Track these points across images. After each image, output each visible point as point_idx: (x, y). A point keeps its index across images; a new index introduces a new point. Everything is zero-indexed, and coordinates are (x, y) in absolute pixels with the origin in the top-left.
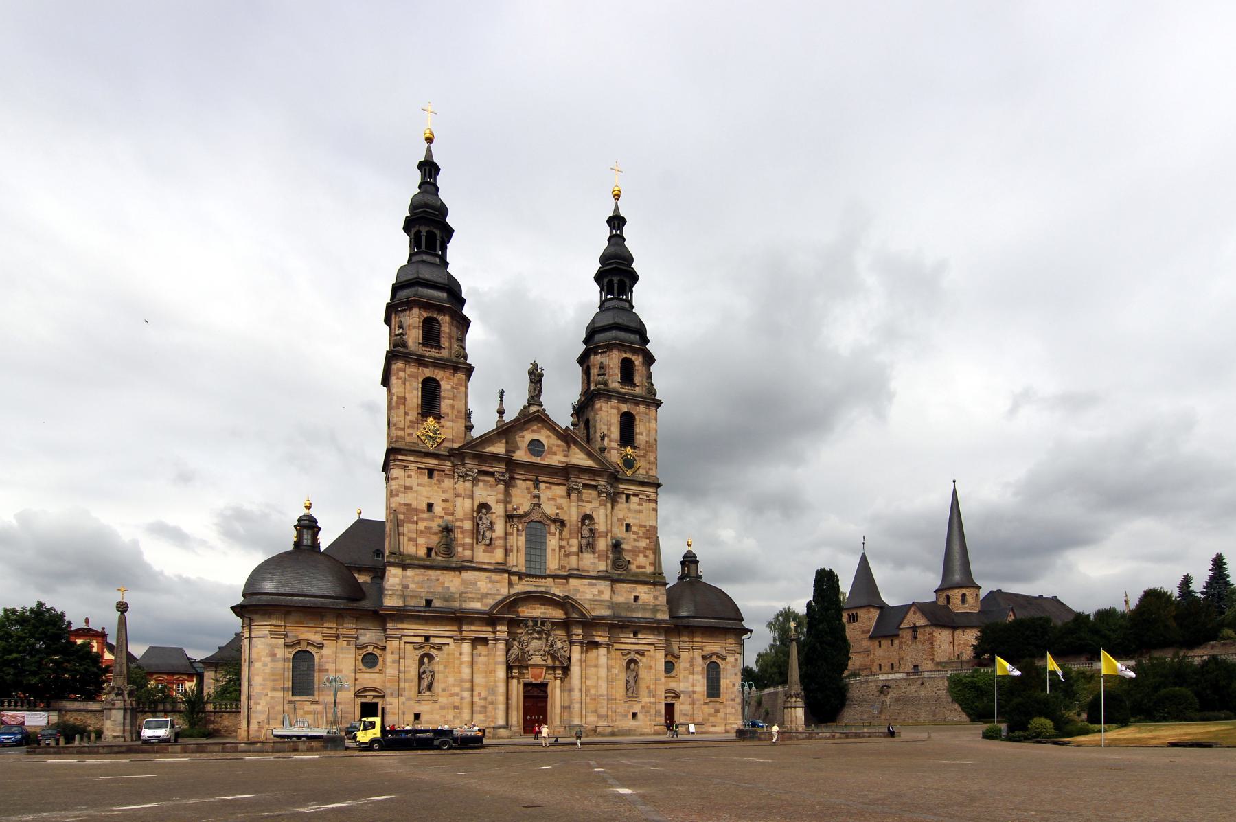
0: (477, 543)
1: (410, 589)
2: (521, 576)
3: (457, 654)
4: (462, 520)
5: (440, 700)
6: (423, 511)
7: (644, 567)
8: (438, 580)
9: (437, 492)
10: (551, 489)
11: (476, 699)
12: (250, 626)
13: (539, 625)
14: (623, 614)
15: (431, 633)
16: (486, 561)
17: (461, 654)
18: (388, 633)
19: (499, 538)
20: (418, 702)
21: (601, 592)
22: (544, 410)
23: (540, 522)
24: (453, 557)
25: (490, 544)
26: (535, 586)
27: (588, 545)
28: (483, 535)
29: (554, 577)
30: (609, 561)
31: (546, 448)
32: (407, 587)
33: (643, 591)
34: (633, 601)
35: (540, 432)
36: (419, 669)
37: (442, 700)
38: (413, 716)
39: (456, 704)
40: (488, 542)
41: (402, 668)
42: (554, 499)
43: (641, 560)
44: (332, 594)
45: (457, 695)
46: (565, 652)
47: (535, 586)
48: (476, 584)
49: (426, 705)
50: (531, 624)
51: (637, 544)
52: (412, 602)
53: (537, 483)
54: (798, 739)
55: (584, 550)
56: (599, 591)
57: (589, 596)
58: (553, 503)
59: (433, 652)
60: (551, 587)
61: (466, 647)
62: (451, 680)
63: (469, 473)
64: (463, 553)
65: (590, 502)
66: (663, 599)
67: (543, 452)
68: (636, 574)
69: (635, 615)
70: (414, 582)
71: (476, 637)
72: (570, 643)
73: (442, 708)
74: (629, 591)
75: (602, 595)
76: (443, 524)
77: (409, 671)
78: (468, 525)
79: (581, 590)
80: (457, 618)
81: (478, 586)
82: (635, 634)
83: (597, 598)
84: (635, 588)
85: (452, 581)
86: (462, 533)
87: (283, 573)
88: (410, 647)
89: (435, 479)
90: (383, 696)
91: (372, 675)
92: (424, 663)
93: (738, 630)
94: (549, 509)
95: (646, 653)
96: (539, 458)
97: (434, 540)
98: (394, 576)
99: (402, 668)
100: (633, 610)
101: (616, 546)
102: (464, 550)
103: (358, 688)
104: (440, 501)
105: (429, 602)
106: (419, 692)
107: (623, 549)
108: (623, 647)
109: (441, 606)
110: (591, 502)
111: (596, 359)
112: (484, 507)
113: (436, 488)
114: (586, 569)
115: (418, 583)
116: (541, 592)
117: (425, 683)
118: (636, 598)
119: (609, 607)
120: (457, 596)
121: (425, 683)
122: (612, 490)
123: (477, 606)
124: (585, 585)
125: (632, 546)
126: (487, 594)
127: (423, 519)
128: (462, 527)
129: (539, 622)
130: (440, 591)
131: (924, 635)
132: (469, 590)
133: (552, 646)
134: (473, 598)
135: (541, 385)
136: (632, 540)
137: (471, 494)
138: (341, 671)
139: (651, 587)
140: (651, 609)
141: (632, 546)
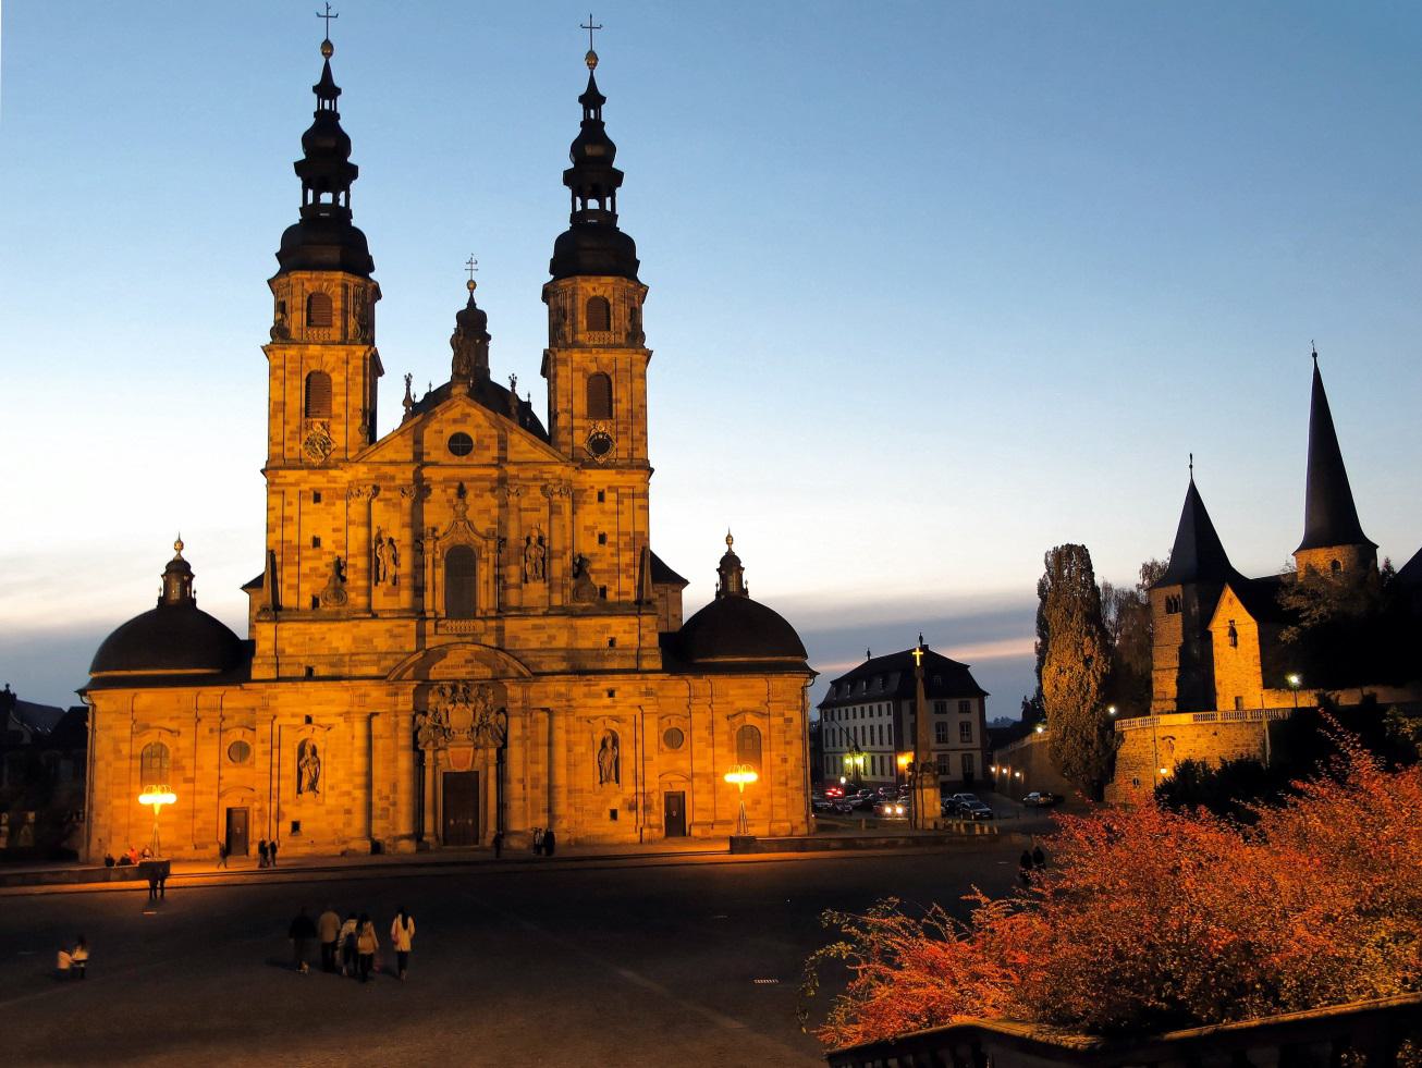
0: (376, 584)
3: (349, 738)
4: (354, 556)
6: (307, 548)
7: (628, 593)
8: (323, 639)
10: (482, 496)
11: (375, 798)
14: (590, 665)
17: (353, 737)
19: (405, 575)
20: (299, 805)
21: (552, 638)
24: (343, 605)
25: (394, 584)
26: (459, 635)
30: (568, 592)
31: (475, 442)
32: (283, 651)
33: (621, 629)
34: (606, 644)
35: (465, 422)
36: (299, 760)
37: (331, 801)
39: (346, 807)
40: (390, 583)
41: (275, 760)
47: (459, 635)
48: (372, 642)
50: (448, 691)
51: (615, 560)
52: (286, 672)
53: (461, 492)
56: (549, 637)
57: (534, 645)
58: (487, 516)
65: (538, 510)
70: (291, 645)
77: (286, 765)
78: (361, 563)
79: (522, 637)
82: (611, 694)
83: (548, 646)
85: (343, 639)
86: (355, 573)
89: (323, 503)
96: (465, 457)
97: (324, 582)
98: (265, 639)
99: (275, 760)
101: (580, 567)
102: (357, 595)
103: (222, 788)
105: (310, 670)
106: (300, 792)
107: (593, 571)
108: (593, 713)
109: (326, 674)
115: (296, 645)
116: (468, 643)
117: (306, 782)
118: (612, 642)
119: (564, 659)
120: (347, 659)
121: (306, 782)
123: (373, 671)
124: (527, 630)
126: (387, 653)
130: (327, 653)
132: (361, 650)
136: (608, 555)
137: (363, 519)
138: (201, 768)
139: (636, 620)
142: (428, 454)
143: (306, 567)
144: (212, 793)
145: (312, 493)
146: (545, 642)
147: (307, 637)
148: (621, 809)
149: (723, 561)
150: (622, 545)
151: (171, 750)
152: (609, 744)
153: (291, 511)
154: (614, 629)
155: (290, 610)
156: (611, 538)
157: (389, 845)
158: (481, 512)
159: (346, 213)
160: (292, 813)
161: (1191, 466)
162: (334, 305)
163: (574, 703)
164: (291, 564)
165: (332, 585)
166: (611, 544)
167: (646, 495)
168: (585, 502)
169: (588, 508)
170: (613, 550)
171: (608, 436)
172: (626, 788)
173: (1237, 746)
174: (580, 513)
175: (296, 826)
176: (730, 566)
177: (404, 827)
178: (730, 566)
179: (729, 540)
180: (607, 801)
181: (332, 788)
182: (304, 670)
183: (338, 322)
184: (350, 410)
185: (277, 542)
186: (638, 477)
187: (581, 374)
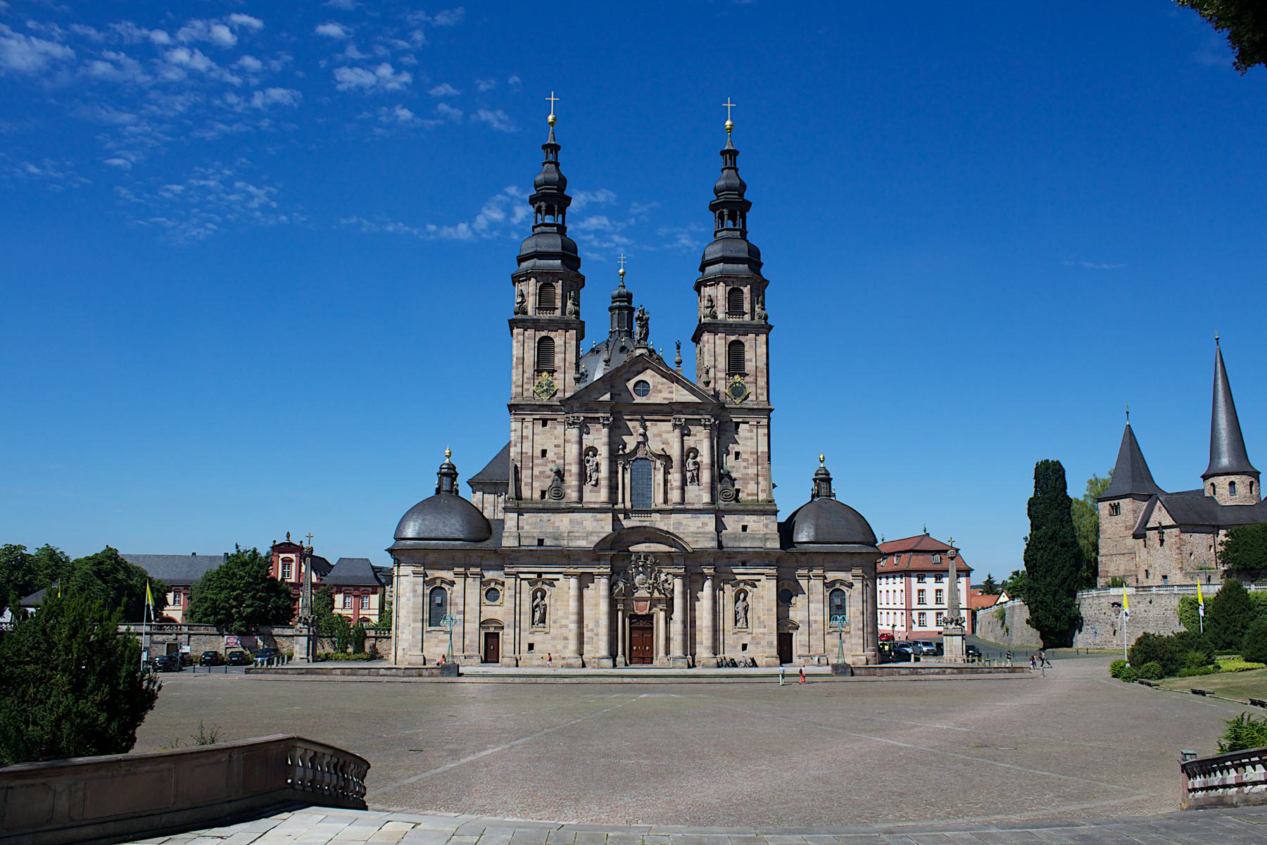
1: (525, 530)
2: (627, 513)
4: (571, 464)
8: (549, 520)
9: (551, 439)
10: (656, 425)
12: (399, 566)
13: (642, 560)
18: (506, 570)
20: (531, 633)
21: (704, 524)
23: (646, 459)
25: (596, 485)
26: (640, 521)
28: (591, 477)
29: (658, 511)
32: (523, 528)
36: (533, 601)
38: (527, 646)
39: (565, 635)
40: (594, 483)
43: (752, 487)
44: (462, 536)
45: (566, 626)
46: (669, 584)
47: (640, 521)
49: (539, 635)
52: (524, 542)
54: (899, 674)
55: (688, 483)
56: (703, 523)
57: (693, 529)
58: (659, 439)
59: (546, 587)
60: (656, 521)
61: (573, 582)
62: (560, 613)
63: (576, 421)
64: (572, 495)
68: (746, 503)
71: (582, 573)
73: (553, 639)
74: (737, 521)
75: (706, 528)
76: (555, 469)
78: (575, 469)
79: (684, 523)
80: (566, 557)
81: (584, 525)
83: (701, 530)
84: (743, 520)
85: (562, 521)
86: (570, 476)
87: (423, 520)
88: (525, 583)
89: (548, 427)
90: (503, 628)
91: (494, 607)
92: (537, 597)
93: (864, 555)
94: (655, 446)
95: (756, 583)
96: (644, 397)
97: (548, 482)
98: (511, 519)
100: (741, 540)
101: (721, 477)
103: (482, 621)
105: (541, 542)
106: (533, 624)
110: (696, 436)
111: (707, 291)
113: (549, 435)
114: (691, 501)
115: (531, 524)
116: (645, 527)
117: (537, 615)
118: (744, 528)
120: (566, 534)
121: (537, 615)
122: (717, 422)
123: (583, 543)
124: (688, 518)
125: (742, 474)
127: (538, 465)
128: (571, 471)
129: (642, 556)
130: (552, 531)
131: (1170, 537)
132: (575, 529)
133: (656, 579)
134: (580, 537)
135: (647, 328)
140: (759, 538)
141: (742, 474)
142: (620, 395)
143: (536, 472)
144: (475, 622)
145: (541, 421)
146: (700, 527)
147: (539, 519)
148: (751, 644)
150: (751, 461)
151: (449, 592)
152: (742, 596)
153: (526, 432)
155: (526, 499)
156: (744, 456)
157: (594, 662)
158: (655, 436)
160: (532, 639)
161: (1127, 412)
162: (557, 291)
163: (717, 570)
164: (527, 469)
166: (744, 460)
167: (769, 426)
168: (726, 431)
169: (728, 434)
170: (745, 464)
171: (742, 385)
172: (754, 629)
173: (1166, 610)
174: (722, 437)
175: (531, 647)
176: (824, 479)
177: (604, 651)
178: (824, 479)
180: (742, 638)
182: (537, 541)
183: (559, 304)
184: (567, 365)
185: (518, 453)
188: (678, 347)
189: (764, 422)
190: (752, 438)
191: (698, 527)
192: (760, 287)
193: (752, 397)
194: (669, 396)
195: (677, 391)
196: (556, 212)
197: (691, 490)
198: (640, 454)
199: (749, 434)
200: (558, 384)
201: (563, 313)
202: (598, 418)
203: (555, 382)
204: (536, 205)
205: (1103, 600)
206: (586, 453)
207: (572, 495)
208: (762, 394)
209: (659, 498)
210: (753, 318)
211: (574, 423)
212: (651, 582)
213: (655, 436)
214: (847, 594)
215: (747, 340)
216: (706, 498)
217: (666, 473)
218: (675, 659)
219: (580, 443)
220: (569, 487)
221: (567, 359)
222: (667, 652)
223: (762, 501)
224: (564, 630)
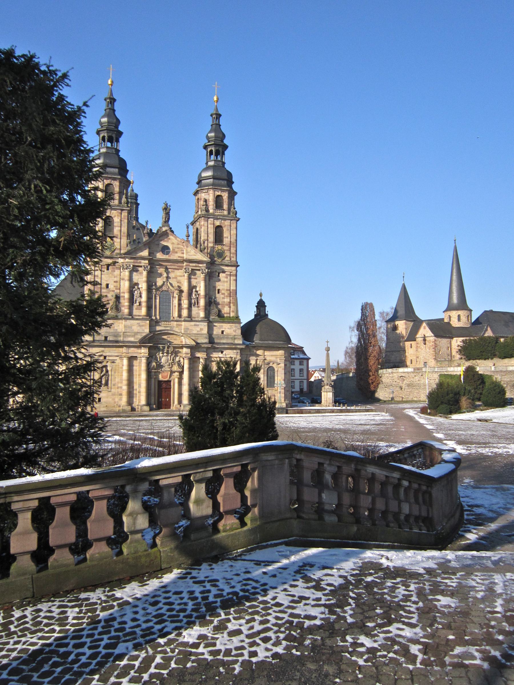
4: (124, 293)
5: (112, 390)
9: (112, 277)
10: (174, 272)
15: (107, 354)
16: (138, 314)
21: (201, 329)
22: (171, 228)
25: (140, 305)
26: (165, 327)
27: (195, 302)
28: (136, 300)
31: (171, 250)
33: (227, 327)
40: (138, 304)
42: (176, 278)
45: (121, 387)
48: (131, 327)
57: (195, 332)
66: (239, 332)
67: (169, 252)
69: (222, 341)
72: (183, 359)
73: (114, 394)
78: (127, 296)
79: (190, 328)
83: (200, 333)
84: (222, 327)
86: (124, 299)
100: (221, 339)
104: (113, 282)
105: (106, 338)
111: (203, 195)
112: (137, 284)
116: (168, 330)
118: (222, 332)
119: (206, 338)
120: (122, 334)
123: (132, 339)
126: (138, 333)
128: (124, 297)
132: (128, 331)
133: (173, 360)
140: (232, 338)
149: (258, 303)
150: (226, 294)
154: (224, 327)
156: (223, 292)
158: (173, 278)
159: (117, 151)
165: (115, 304)
166: (223, 294)
168: (213, 277)
169: (214, 279)
170: (223, 296)
174: (211, 280)
176: (261, 305)
177: (143, 401)
178: (261, 305)
179: (261, 295)
181: (114, 385)
184: (122, 234)
186: (234, 268)
187: (212, 226)
188: (188, 227)
189: (234, 272)
190: (227, 282)
191: (198, 331)
192: (232, 194)
193: (227, 259)
194: (182, 255)
195: (187, 252)
196: (114, 141)
197: (194, 309)
198: (164, 288)
199: (226, 279)
200: (117, 245)
201: (120, 202)
202: (141, 266)
203: (115, 244)
204: (101, 136)
205: (395, 374)
206: (133, 286)
207: (126, 311)
208: (233, 257)
209: (176, 314)
210: (229, 213)
211: (127, 269)
212: (170, 362)
213: (173, 278)
214: (276, 369)
215: (225, 226)
216: (202, 314)
217: (180, 300)
218: (185, 406)
219: (131, 279)
220: (124, 306)
221: (122, 231)
222: (180, 402)
223: (233, 317)
224: (119, 390)
